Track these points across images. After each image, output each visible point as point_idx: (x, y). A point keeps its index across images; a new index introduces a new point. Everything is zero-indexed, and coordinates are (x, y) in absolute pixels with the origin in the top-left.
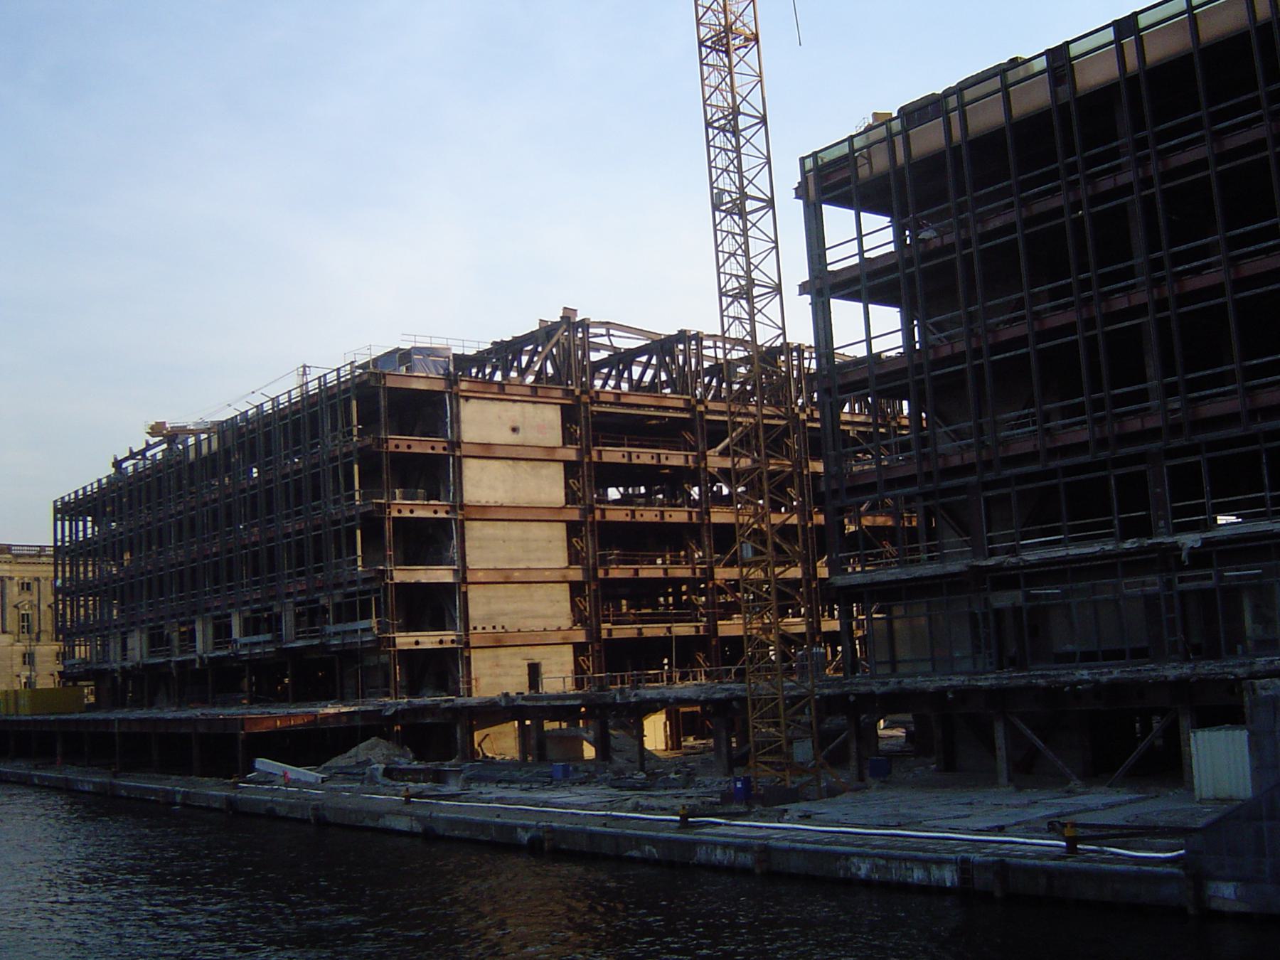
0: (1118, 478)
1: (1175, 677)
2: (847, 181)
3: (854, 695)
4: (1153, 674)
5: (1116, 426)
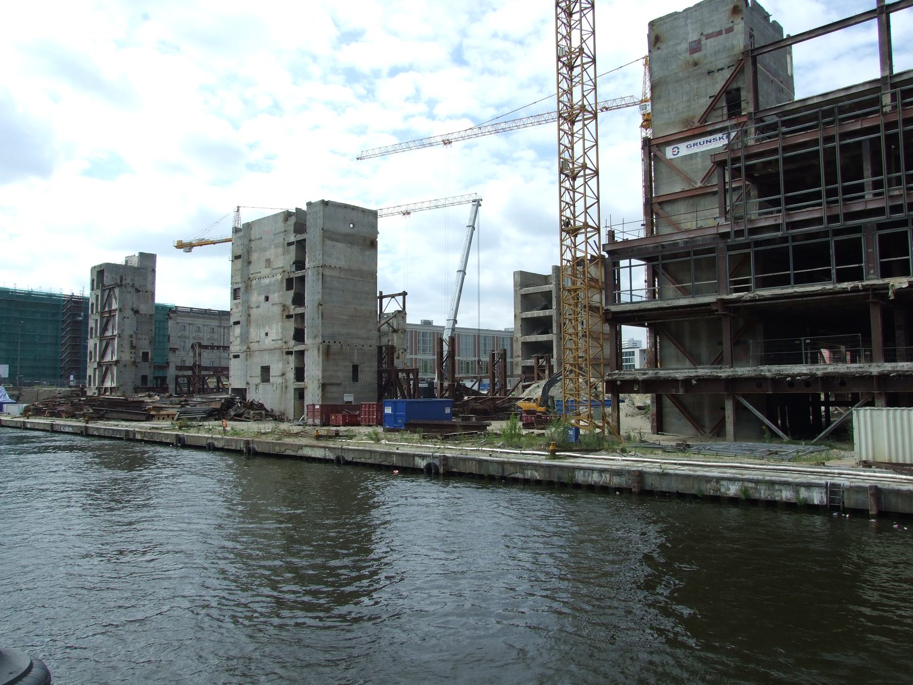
1: (879, 373)
3: (620, 381)
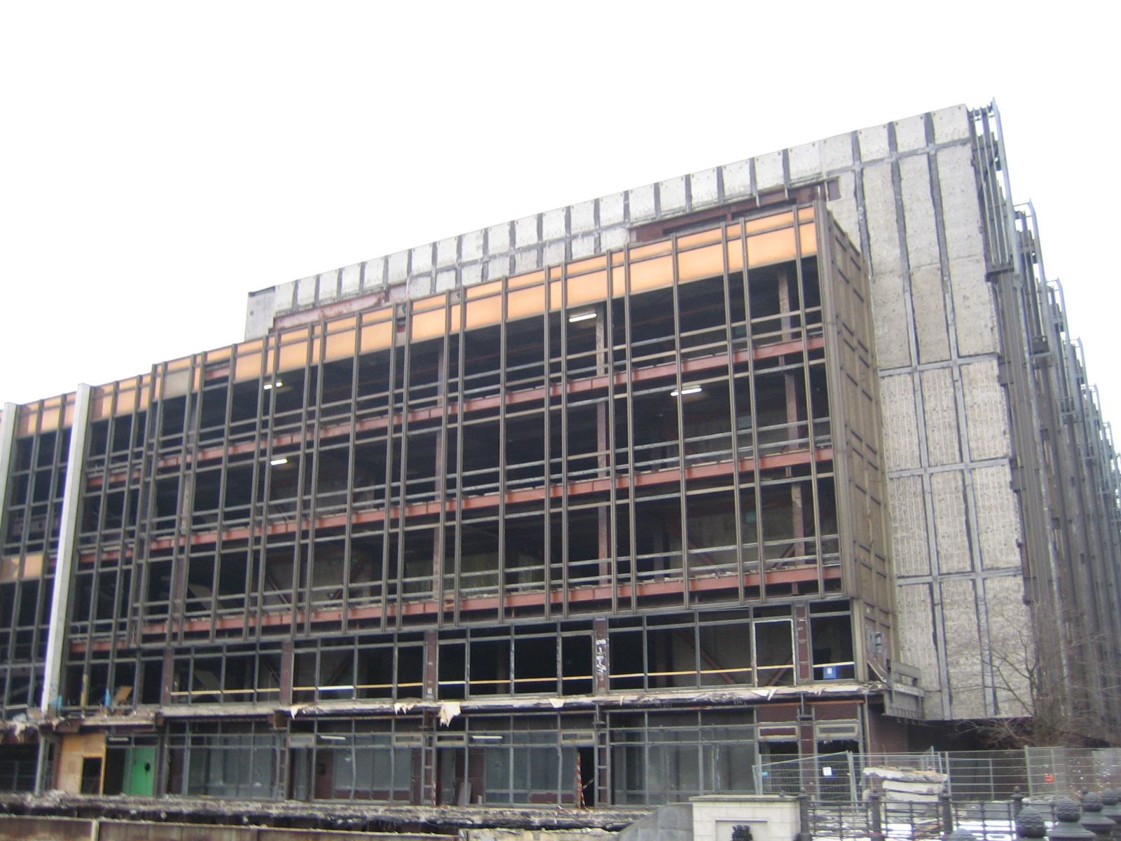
0: (400, 650)
2: (225, 379)
4: (409, 815)
5: (404, 608)
